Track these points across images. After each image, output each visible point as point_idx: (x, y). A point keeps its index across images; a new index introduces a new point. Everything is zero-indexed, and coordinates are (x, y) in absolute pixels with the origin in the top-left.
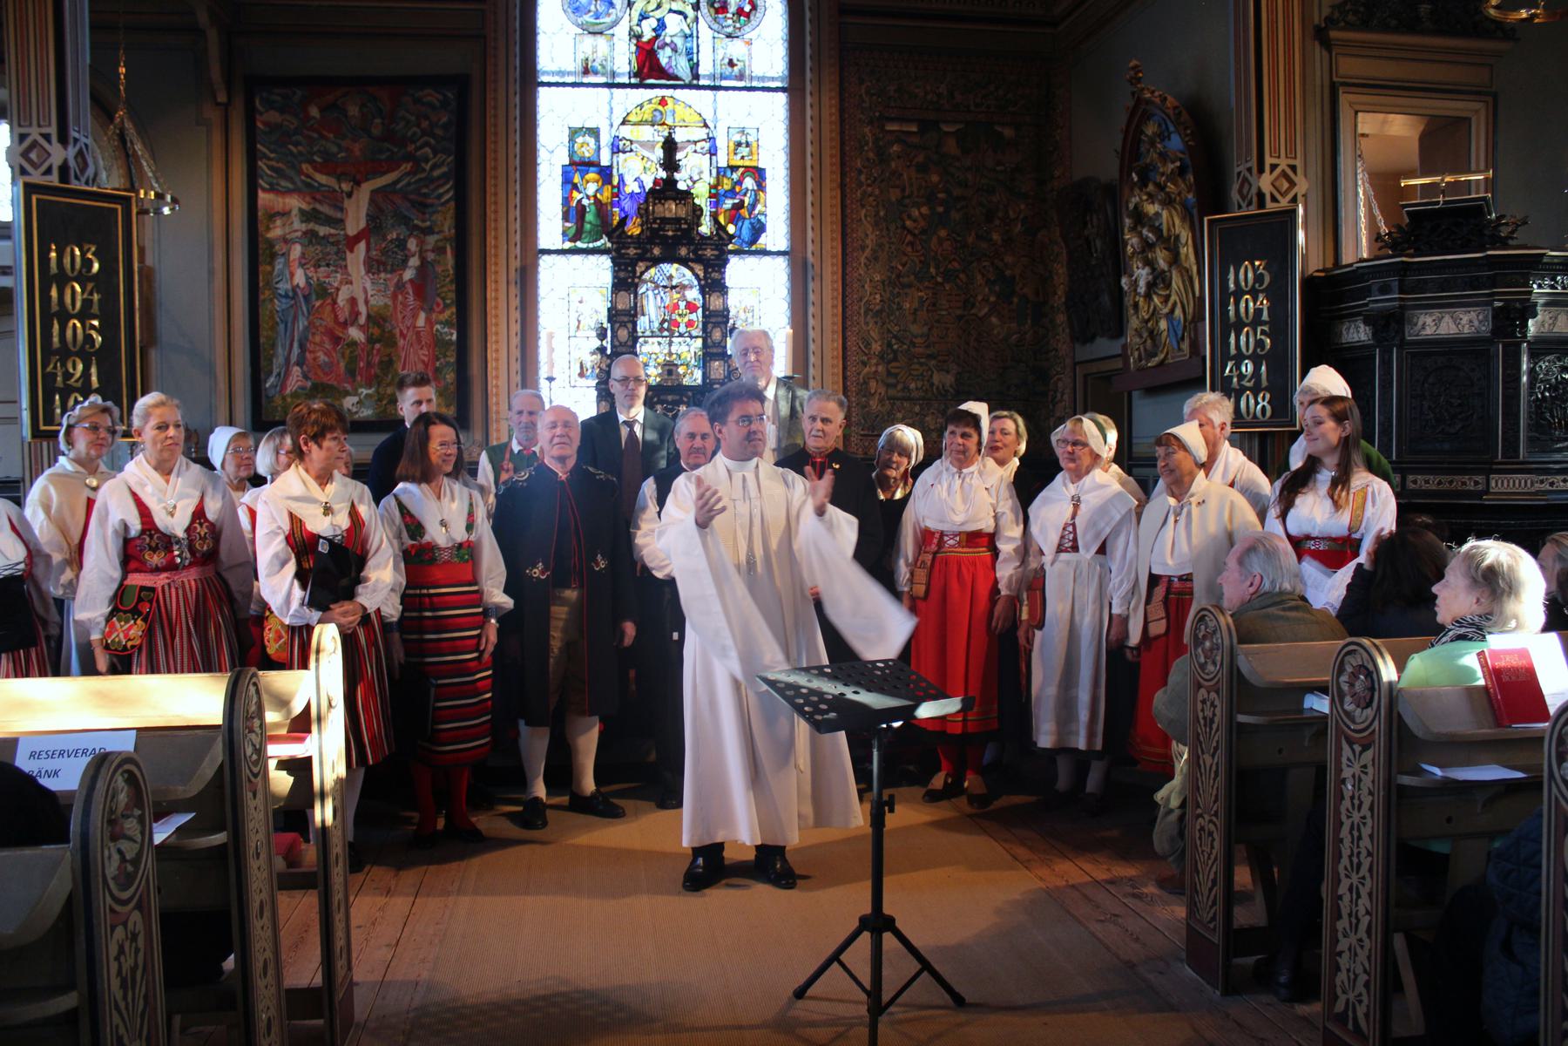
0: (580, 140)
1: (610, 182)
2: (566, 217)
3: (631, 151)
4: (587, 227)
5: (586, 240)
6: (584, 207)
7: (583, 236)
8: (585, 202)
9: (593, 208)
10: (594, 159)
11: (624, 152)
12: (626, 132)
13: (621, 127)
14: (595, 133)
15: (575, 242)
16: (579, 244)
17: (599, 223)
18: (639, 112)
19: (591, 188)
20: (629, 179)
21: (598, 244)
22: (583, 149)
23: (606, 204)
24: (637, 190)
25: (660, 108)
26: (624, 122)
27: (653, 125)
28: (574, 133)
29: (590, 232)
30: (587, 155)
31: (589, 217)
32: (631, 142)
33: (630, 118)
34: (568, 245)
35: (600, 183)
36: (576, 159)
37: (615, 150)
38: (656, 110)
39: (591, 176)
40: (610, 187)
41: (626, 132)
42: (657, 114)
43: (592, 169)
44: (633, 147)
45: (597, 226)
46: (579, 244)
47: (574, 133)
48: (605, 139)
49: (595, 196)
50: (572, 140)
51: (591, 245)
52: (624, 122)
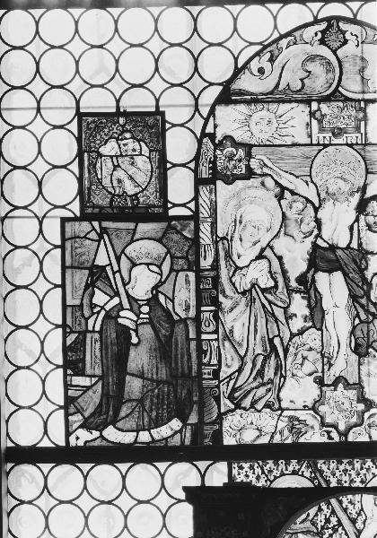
0: (110, 148)
1: (194, 266)
2: (73, 363)
3: (250, 174)
4: (134, 386)
5: (131, 423)
6: (124, 332)
7: (124, 411)
8: (127, 318)
9: (147, 331)
10: (150, 197)
11: (229, 180)
12: (230, 121)
13: (220, 110)
14: (151, 126)
15: (101, 427)
16: (112, 434)
17: (163, 374)
18: (267, 66)
19: (143, 283)
20: (244, 252)
21: (163, 432)
22: (119, 174)
23: (184, 321)
24: (266, 282)
25: (324, 51)
26: (228, 96)
27: (308, 102)
28: (91, 128)
29: (141, 401)
30: (130, 189)
31: (139, 358)
32: (248, 148)
33: (247, 83)
34: (83, 437)
35: (166, 267)
36: (100, 199)
37: (205, 173)
38: (312, 58)
39: (146, 248)
40: (192, 276)
41: (230, 121)
42: (315, 68)
43: (144, 228)
44: (254, 164)
45: (159, 382)
46: (112, 434)
47: (91, 128)
48: (180, 146)
49: (153, 301)
50: (87, 151)
51: (144, 437)
52: (228, 96)
